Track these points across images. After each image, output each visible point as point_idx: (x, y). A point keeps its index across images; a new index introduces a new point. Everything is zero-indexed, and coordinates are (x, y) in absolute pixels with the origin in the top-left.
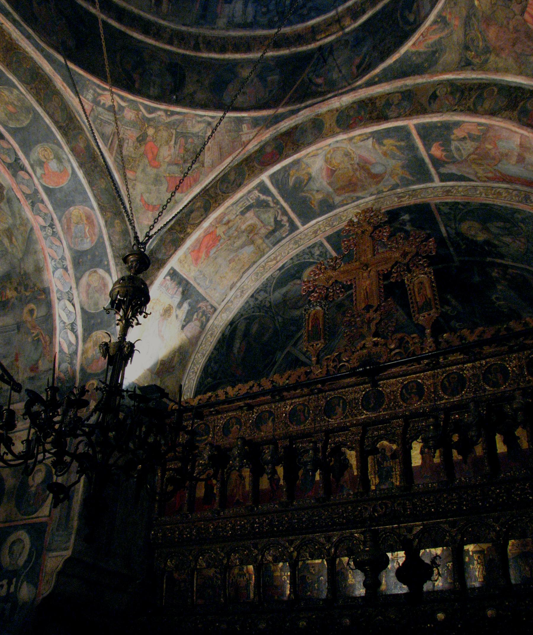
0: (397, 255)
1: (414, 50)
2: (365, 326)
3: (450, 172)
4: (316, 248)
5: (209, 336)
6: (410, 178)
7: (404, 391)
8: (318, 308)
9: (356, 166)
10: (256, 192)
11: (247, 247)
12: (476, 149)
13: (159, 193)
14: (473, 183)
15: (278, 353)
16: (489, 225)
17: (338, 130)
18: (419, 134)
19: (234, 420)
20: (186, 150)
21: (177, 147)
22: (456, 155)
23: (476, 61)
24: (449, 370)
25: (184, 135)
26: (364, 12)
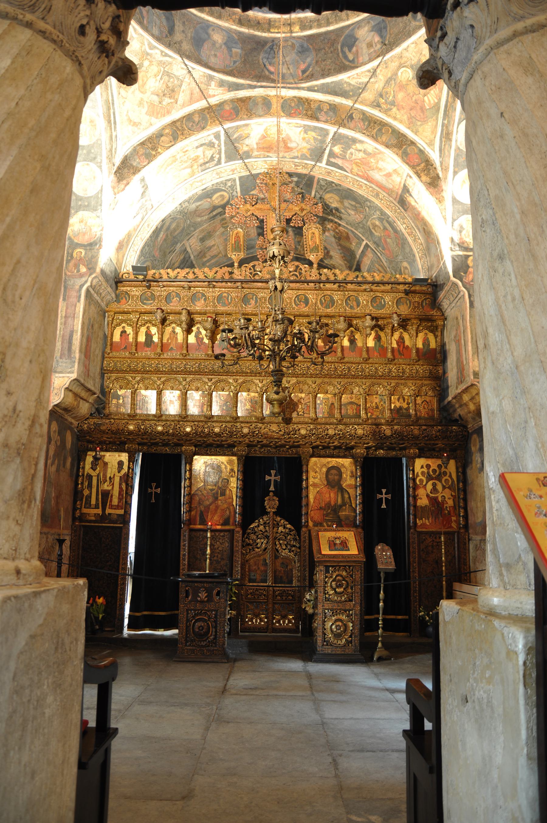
0: (297, 209)
1: (348, 80)
8: (240, 230)
15: (179, 244)
16: (345, 200)
17: (282, 114)
20: (167, 87)
21: (162, 82)
22: (347, 156)
23: (384, 106)
25: (168, 74)
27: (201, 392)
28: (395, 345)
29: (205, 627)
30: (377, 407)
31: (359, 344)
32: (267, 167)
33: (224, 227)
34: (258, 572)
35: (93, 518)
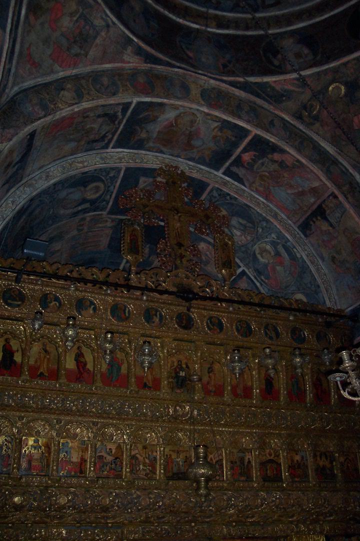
1: (273, 85)
3: (237, 172)
4: (114, 171)
5: (10, 202)
6: (207, 161)
8: (136, 227)
9: (188, 132)
10: (121, 107)
12: (275, 171)
13: (44, 54)
14: (243, 187)
18: (251, 141)
22: (255, 168)
26: (228, 28)
32: (158, 162)
33: (78, 230)
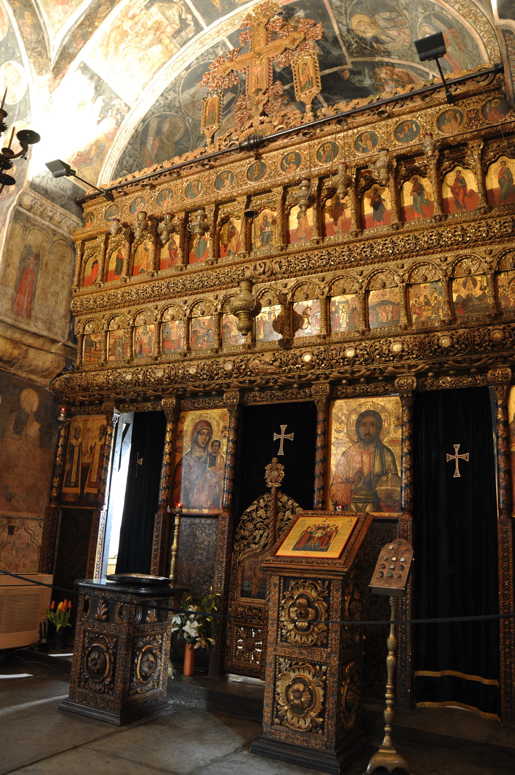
2: (254, 108)
4: (220, 48)
7: (284, 161)
8: (215, 96)
11: (154, 46)
19: (139, 199)
24: (325, 140)
27: (177, 322)
28: (448, 194)
29: (99, 661)
30: (428, 303)
31: (389, 205)
34: (255, 581)
35: (71, 499)
